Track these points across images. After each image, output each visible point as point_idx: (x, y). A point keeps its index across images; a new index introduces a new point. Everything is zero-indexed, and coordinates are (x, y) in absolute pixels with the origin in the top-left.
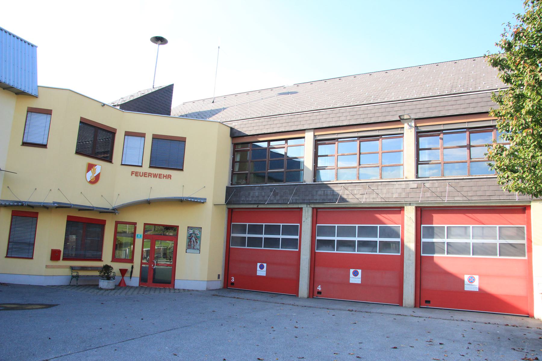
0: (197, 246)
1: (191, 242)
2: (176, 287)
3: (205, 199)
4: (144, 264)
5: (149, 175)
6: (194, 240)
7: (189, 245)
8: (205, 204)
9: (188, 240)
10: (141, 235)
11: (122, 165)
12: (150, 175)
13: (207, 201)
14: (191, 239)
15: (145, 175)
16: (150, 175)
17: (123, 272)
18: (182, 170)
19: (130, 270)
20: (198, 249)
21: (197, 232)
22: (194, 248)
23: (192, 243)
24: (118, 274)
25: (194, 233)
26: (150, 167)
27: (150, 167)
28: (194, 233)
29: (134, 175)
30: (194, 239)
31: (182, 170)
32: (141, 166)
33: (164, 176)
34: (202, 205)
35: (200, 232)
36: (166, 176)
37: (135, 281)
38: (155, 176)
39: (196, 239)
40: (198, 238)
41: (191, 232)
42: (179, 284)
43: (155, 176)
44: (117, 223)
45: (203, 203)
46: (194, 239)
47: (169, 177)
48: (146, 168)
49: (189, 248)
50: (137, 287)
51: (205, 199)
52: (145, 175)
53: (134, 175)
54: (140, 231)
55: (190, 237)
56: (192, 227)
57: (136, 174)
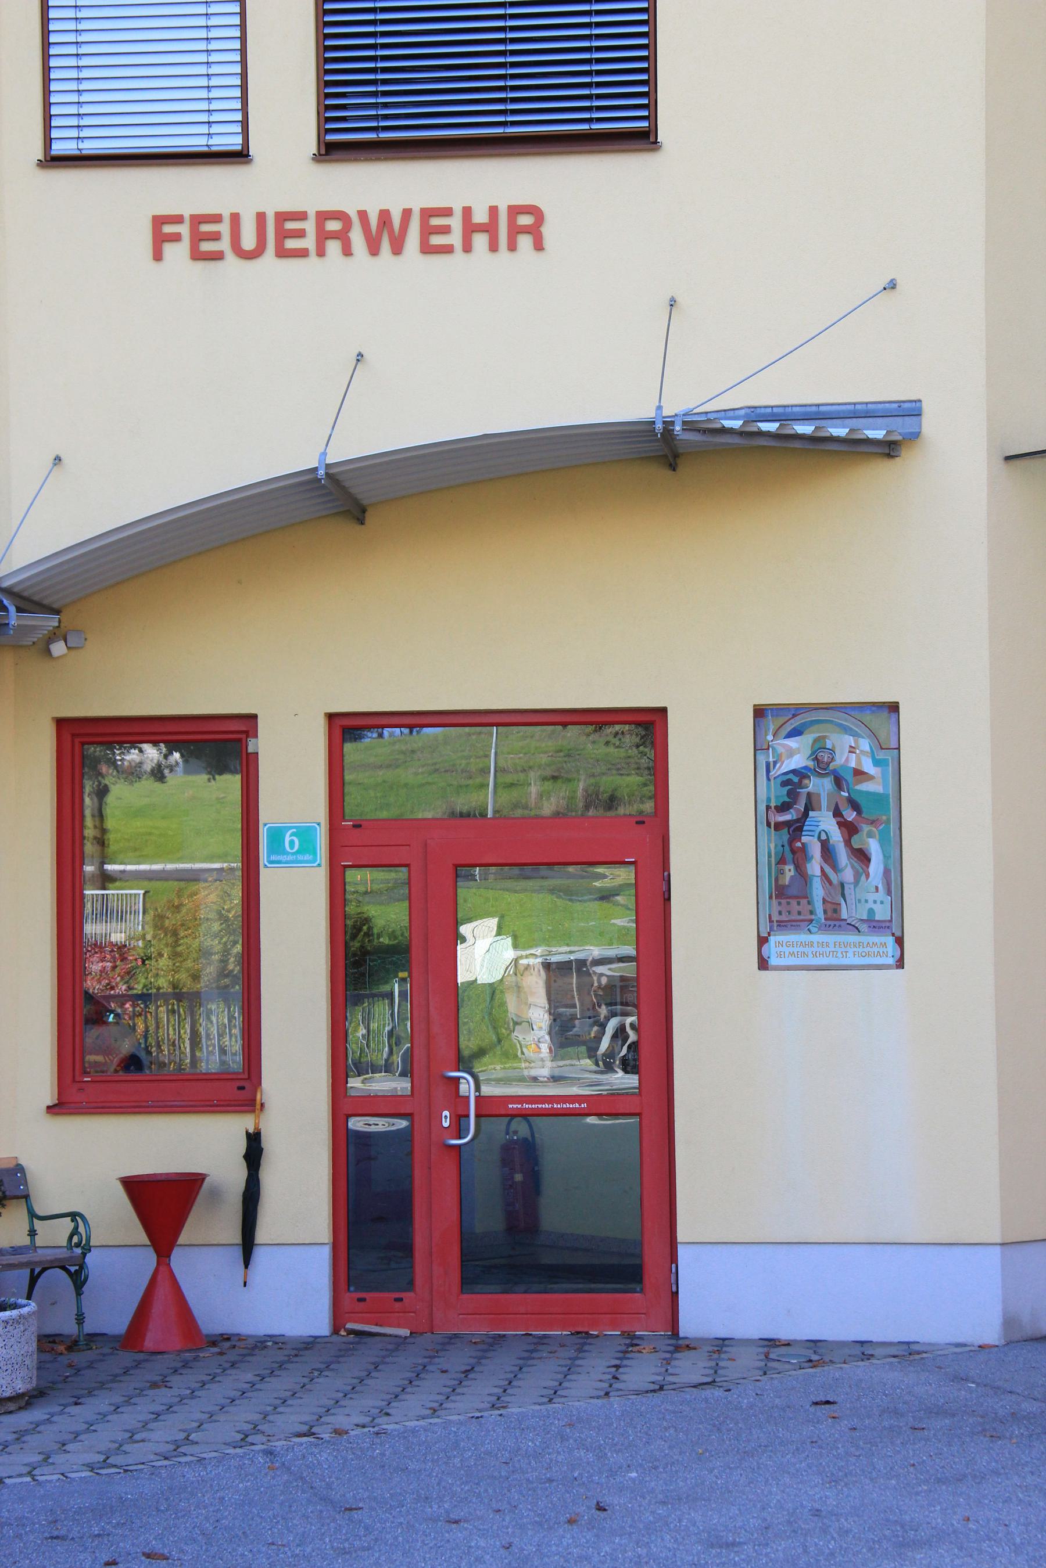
0: (868, 897)
1: (798, 856)
2: (690, 1324)
3: (912, 410)
4: (373, 1106)
5: (323, 237)
6: (828, 832)
7: (780, 892)
8: (909, 465)
9: (772, 842)
10: (305, 834)
11: (53, 161)
12: (333, 229)
13: (929, 424)
14: (796, 828)
15: (283, 234)
16: (333, 229)
17: (162, 1203)
18: (645, 139)
19: (227, 1171)
20: (876, 926)
21: (852, 751)
22: (834, 921)
23: (815, 866)
24: (116, 1223)
25: (821, 762)
26: (330, 150)
27: (330, 150)
28: (821, 762)
29: (177, 253)
30: (825, 822)
31: (645, 139)
32: (240, 156)
33: (470, 228)
34: (882, 470)
35: (889, 750)
36: (490, 228)
37: (287, 1280)
38: (384, 233)
39: (849, 829)
40: (866, 816)
41: (795, 755)
42: (717, 1292)
43: (384, 233)
44: (86, 746)
45: (889, 449)
46: (825, 822)
47: (524, 225)
48: (287, 170)
49: (782, 925)
50: (310, 1344)
51: (912, 410)
52: (283, 234)
53: (177, 253)
54: (293, 784)
55: (786, 817)
56: (797, 710)
57: (203, 238)
